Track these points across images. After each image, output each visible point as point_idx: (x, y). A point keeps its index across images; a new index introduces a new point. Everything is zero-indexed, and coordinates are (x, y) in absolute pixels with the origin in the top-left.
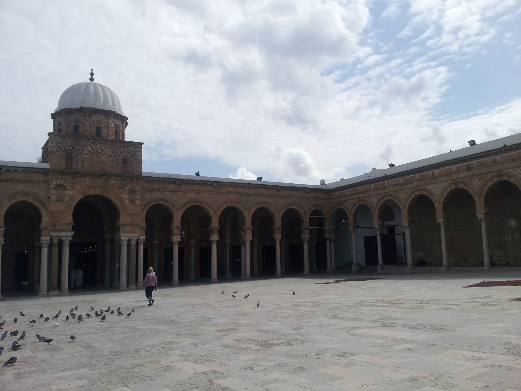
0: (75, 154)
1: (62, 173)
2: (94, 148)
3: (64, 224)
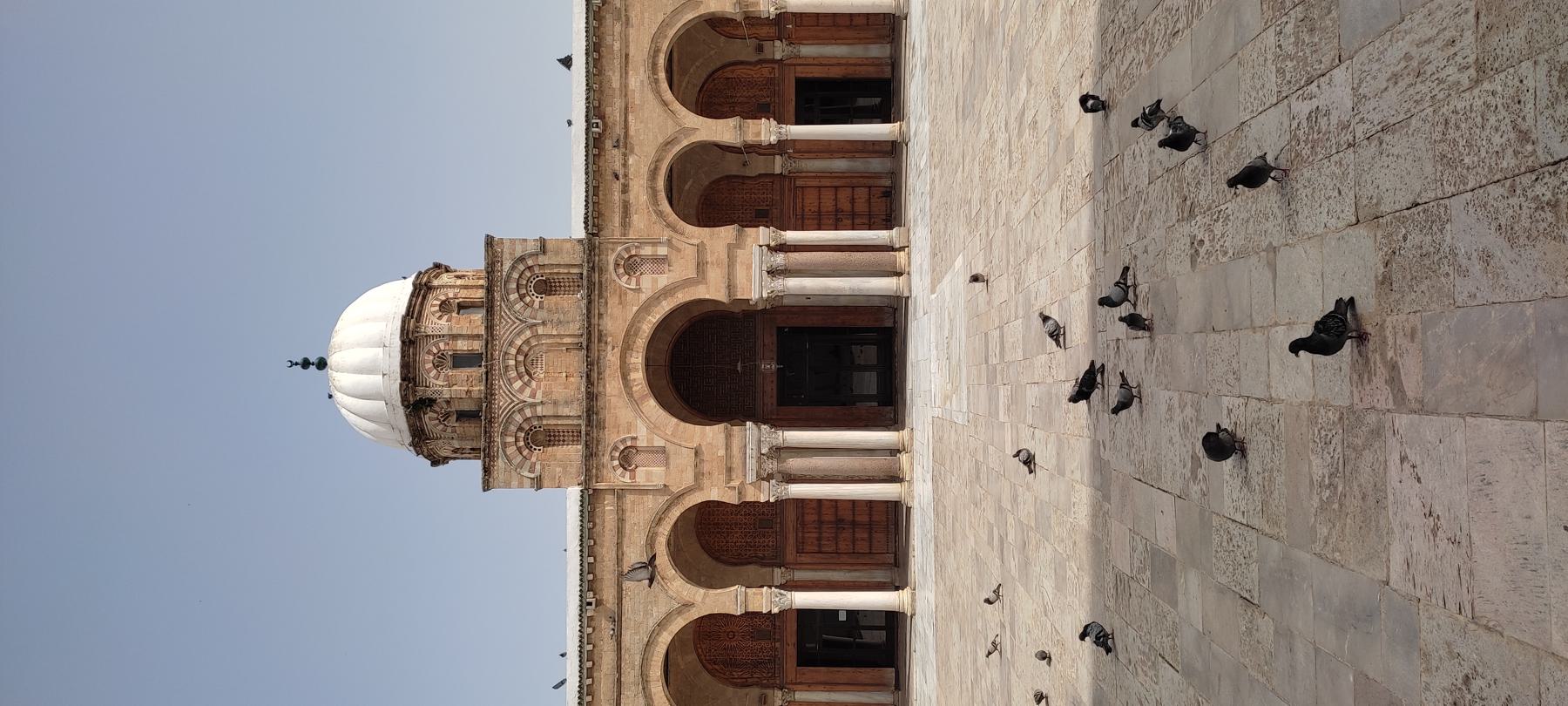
1: (591, 454)
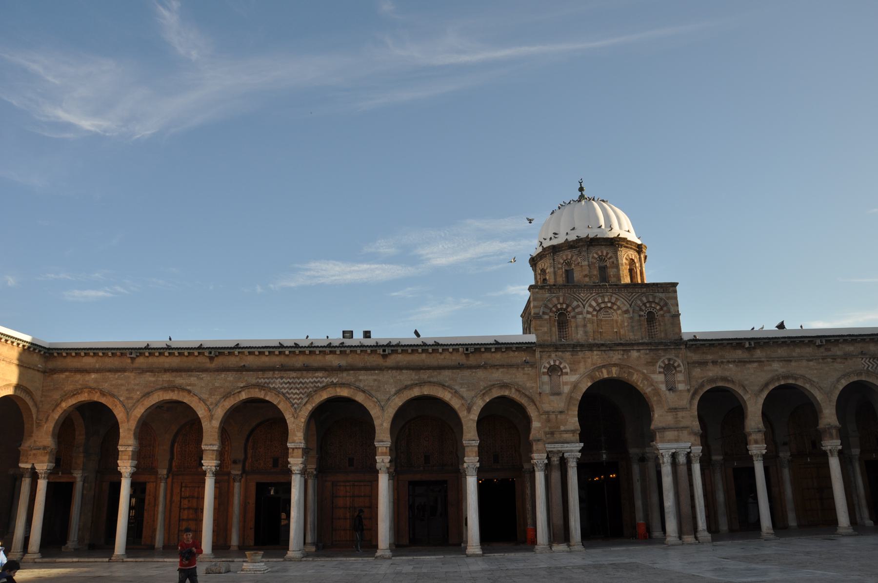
0: (572, 314)
1: (557, 348)
2: (600, 301)
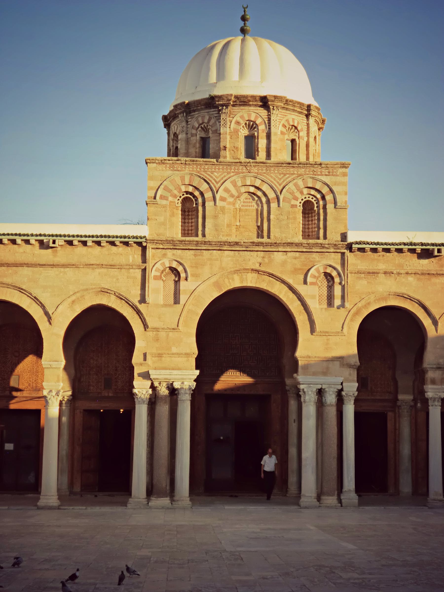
2: (239, 184)
3: (179, 355)
